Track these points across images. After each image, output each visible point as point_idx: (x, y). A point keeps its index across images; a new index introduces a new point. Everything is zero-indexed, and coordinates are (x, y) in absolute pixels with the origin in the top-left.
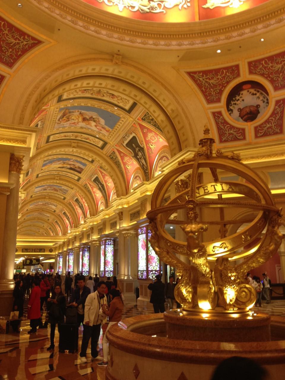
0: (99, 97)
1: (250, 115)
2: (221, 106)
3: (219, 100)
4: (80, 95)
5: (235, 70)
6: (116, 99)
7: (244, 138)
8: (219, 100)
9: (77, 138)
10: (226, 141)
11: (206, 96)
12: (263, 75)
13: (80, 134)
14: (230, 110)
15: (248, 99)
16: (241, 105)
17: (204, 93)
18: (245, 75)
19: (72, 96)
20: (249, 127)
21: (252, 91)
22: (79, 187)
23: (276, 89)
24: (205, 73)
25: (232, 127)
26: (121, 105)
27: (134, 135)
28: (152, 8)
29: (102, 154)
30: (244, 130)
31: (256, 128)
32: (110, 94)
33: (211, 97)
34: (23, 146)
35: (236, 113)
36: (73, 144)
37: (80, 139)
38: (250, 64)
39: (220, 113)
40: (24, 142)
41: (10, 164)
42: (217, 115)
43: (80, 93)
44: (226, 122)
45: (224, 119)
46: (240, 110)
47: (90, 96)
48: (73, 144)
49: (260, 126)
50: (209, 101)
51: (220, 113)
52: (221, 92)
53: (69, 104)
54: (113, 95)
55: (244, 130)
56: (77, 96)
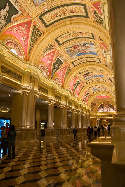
0: (77, 37)
4: (67, 39)
6: (84, 34)
9: (87, 61)
13: (87, 58)
19: (64, 41)
22: (107, 85)
26: (88, 36)
27: (104, 50)
29: (101, 65)
32: (80, 33)
36: (88, 64)
37: (89, 61)
43: (66, 38)
47: (72, 38)
48: (88, 64)
53: (66, 45)
54: (81, 33)
56: (67, 40)
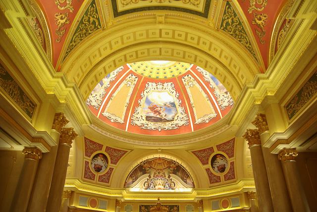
1: (222, 169)
2: (209, 166)
3: (207, 163)
5: (211, 149)
7: (220, 181)
8: (207, 163)
10: (213, 183)
11: (202, 162)
12: (223, 151)
14: (213, 167)
15: (220, 162)
16: (218, 164)
17: (201, 160)
18: (216, 152)
20: (222, 175)
21: (221, 158)
23: (230, 157)
24: (200, 151)
25: (215, 176)
28: (173, 127)
30: (220, 177)
31: (224, 176)
33: (204, 163)
34: (121, 196)
35: (216, 169)
38: (217, 146)
39: (209, 169)
40: (121, 194)
41: (116, 203)
42: (208, 170)
44: (212, 174)
45: (211, 172)
46: (218, 167)
49: (226, 175)
50: (204, 164)
51: (209, 169)
52: (208, 159)
55: (220, 177)
